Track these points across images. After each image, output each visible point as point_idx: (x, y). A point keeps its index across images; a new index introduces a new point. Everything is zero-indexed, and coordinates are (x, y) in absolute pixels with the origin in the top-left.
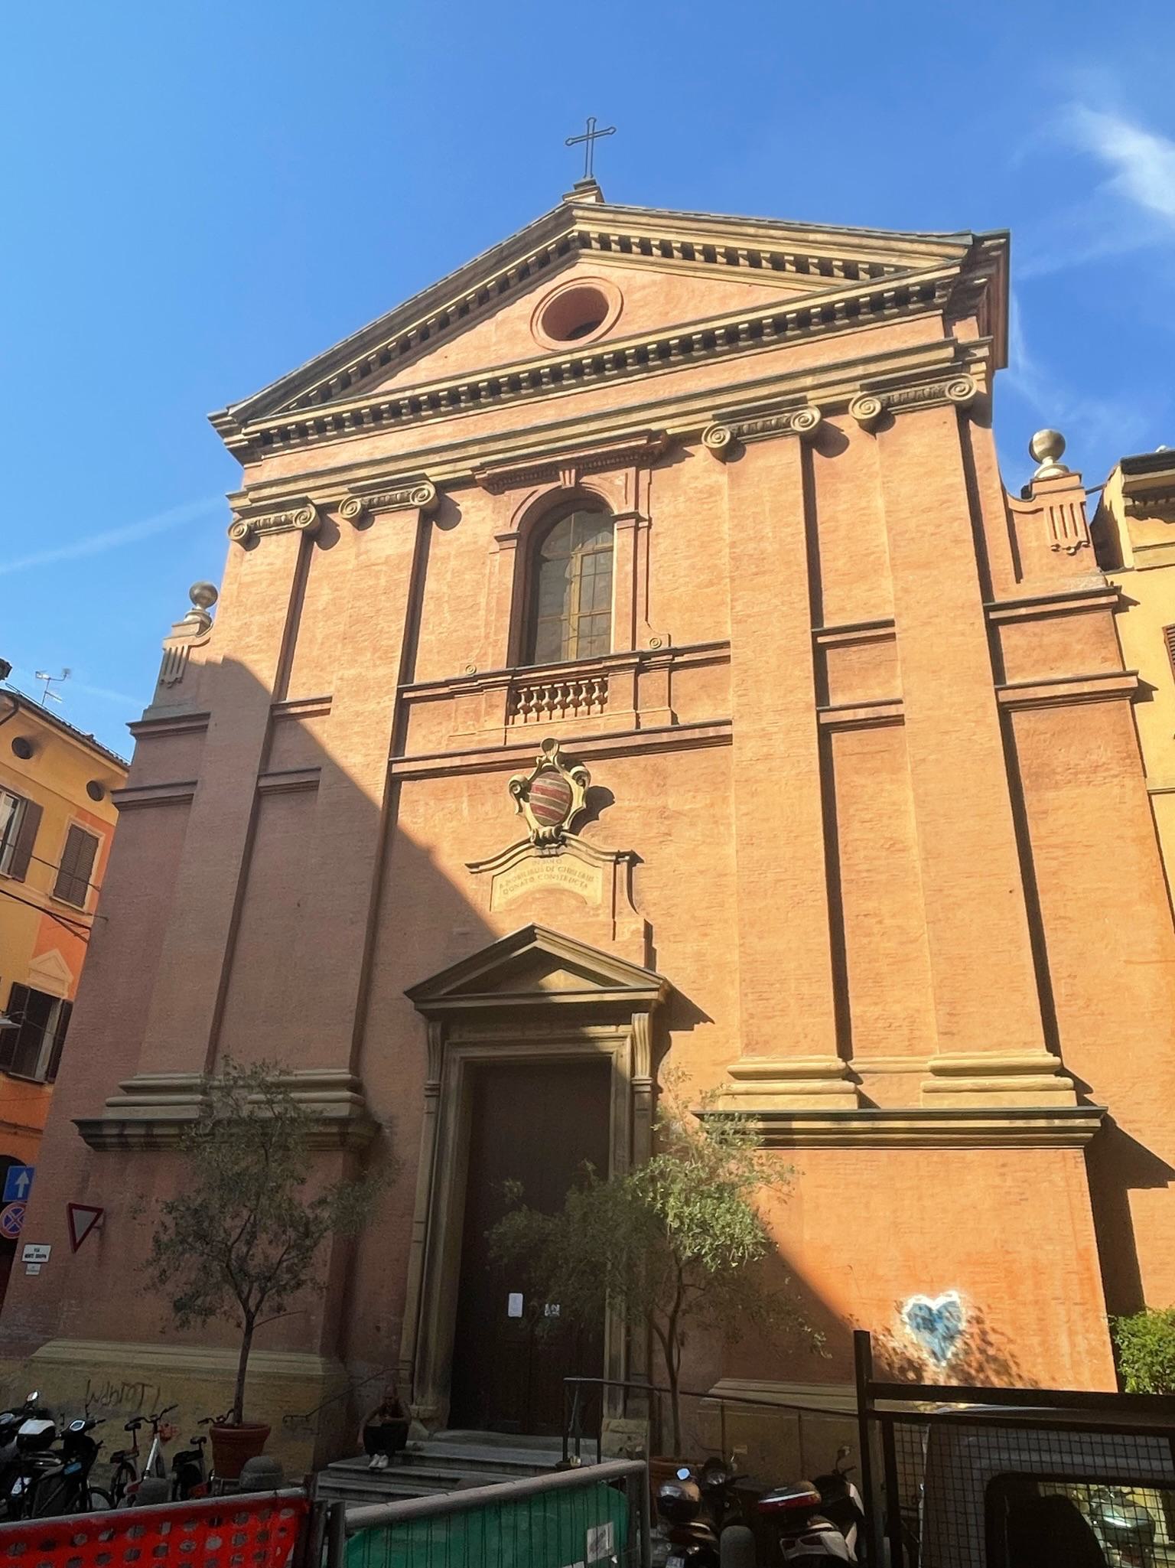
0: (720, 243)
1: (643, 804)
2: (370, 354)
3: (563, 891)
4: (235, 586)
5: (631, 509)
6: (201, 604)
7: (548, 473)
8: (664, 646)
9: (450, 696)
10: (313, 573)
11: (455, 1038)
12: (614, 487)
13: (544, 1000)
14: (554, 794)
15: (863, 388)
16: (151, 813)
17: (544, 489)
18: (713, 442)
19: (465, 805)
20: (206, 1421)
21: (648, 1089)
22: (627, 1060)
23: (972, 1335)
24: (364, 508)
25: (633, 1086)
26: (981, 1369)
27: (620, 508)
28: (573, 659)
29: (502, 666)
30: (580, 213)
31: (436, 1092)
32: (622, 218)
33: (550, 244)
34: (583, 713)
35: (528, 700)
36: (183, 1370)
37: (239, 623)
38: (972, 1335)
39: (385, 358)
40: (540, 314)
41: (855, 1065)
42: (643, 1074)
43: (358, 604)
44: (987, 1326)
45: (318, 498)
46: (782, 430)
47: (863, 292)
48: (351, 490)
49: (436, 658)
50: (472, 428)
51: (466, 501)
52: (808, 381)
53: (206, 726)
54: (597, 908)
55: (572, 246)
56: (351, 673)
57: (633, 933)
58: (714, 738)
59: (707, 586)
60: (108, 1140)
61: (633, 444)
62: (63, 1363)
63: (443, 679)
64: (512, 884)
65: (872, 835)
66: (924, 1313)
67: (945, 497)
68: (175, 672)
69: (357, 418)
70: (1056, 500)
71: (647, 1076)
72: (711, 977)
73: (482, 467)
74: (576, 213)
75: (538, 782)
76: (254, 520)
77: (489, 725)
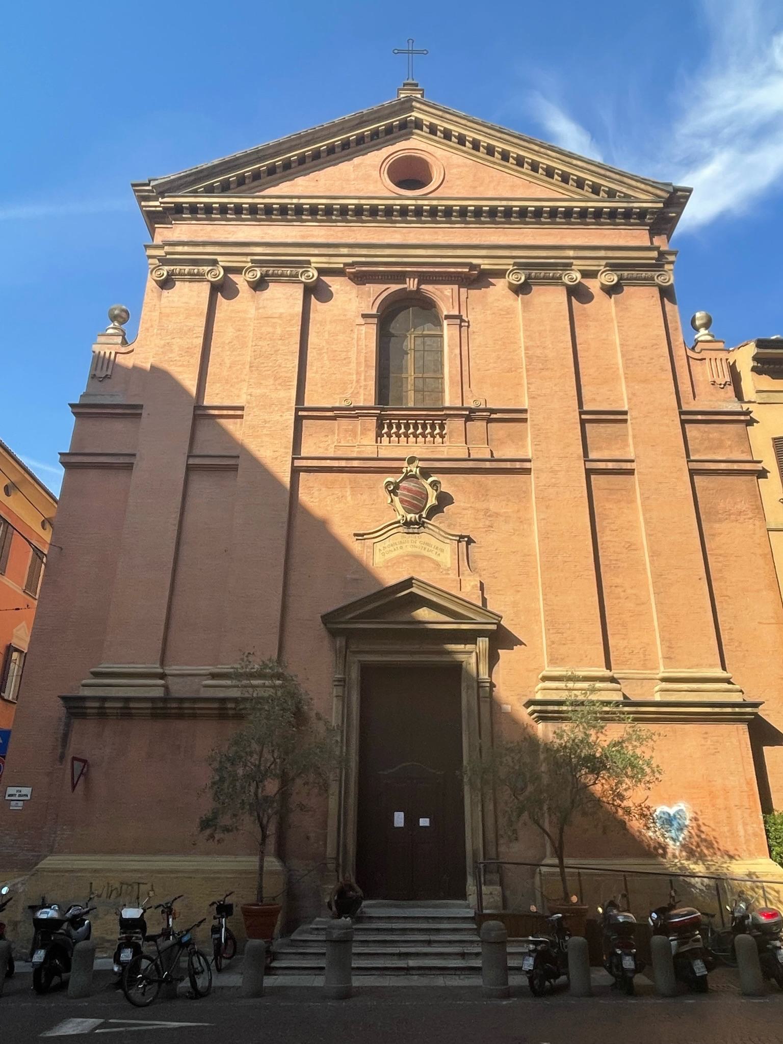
0: (514, 151)
1: (473, 505)
2: (263, 166)
3: (423, 557)
4: (157, 313)
5: (457, 313)
6: (119, 322)
7: (399, 277)
8: (483, 406)
10: (219, 315)
11: (353, 648)
12: (445, 297)
13: (421, 626)
14: (416, 493)
15: (606, 266)
16: (93, 474)
17: (394, 287)
18: (512, 279)
19: (348, 493)
20: (160, 906)
21: (488, 685)
22: (474, 666)
23: (692, 827)
24: (262, 276)
25: (478, 683)
26: (698, 846)
27: (448, 310)
28: (411, 405)
29: (371, 403)
30: (418, 105)
31: (342, 683)
32: (448, 116)
33: (395, 121)
34: (430, 442)
35: (398, 427)
36: (171, 872)
37: (162, 342)
38: (692, 827)
39: (272, 170)
40: (386, 167)
41: (615, 673)
42: (484, 675)
43: (260, 343)
44: (700, 822)
45: (223, 261)
46: (556, 281)
47: (607, 205)
48: (253, 261)
49: (320, 390)
50: (339, 235)
51: (335, 284)
52: (571, 253)
53: (141, 414)
54: (448, 570)
55: (409, 125)
56: (258, 391)
57: (474, 587)
58: (518, 469)
59: (508, 372)
60: (89, 711)
61: (459, 270)
62: (67, 871)
63: (329, 406)
64: (388, 549)
65: (617, 539)
66: (666, 816)
67: (654, 342)
68: (103, 370)
69: (253, 210)
70: (713, 354)
71: (487, 677)
72: (523, 618)
73: (353, 264)
74: (414, 104)
76: (172, 268)
77: (365, 442)
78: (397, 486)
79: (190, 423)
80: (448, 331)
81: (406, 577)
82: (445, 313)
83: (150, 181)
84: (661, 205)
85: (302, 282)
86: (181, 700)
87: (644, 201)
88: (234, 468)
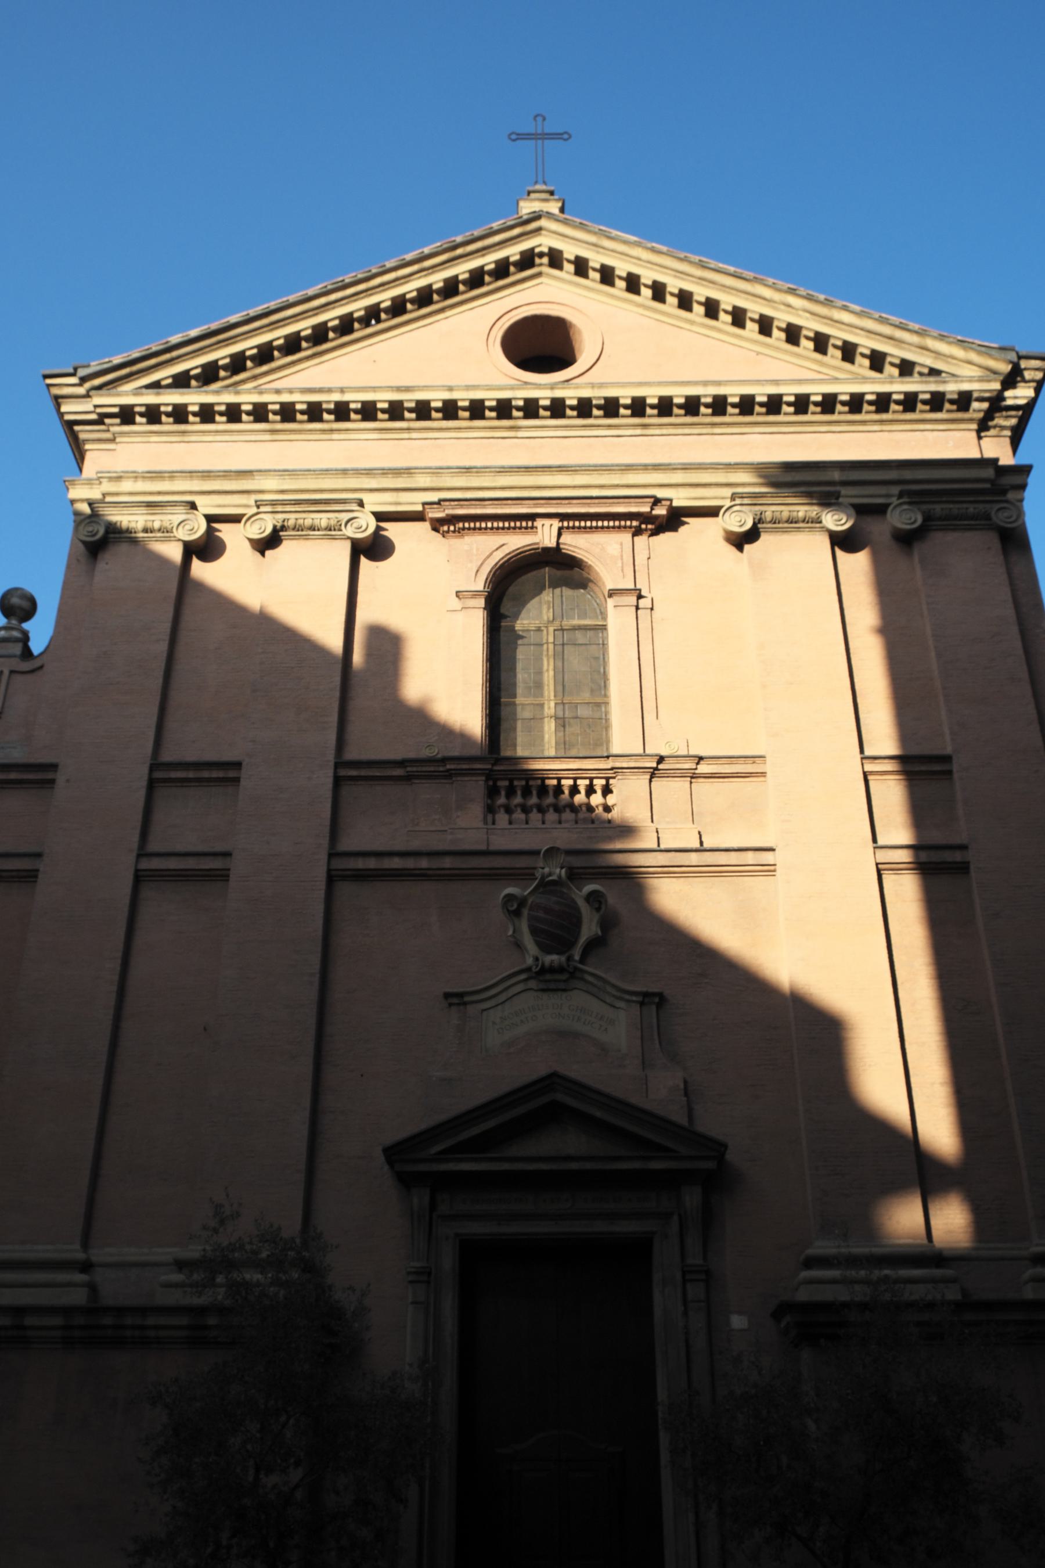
8: (683, 752)
9: (408, 778)
31: (424, 1276)
45: (208, 505)
53: (52, 782)
55: (537, 261)
78: (522, 902)
79: (142, 793)
80: (618, 619)
81: (543, 1071)
82: (610, 585)
83: (76, 369)
85: (349, 538)
86: (120, 1311)
88: (222, 876)
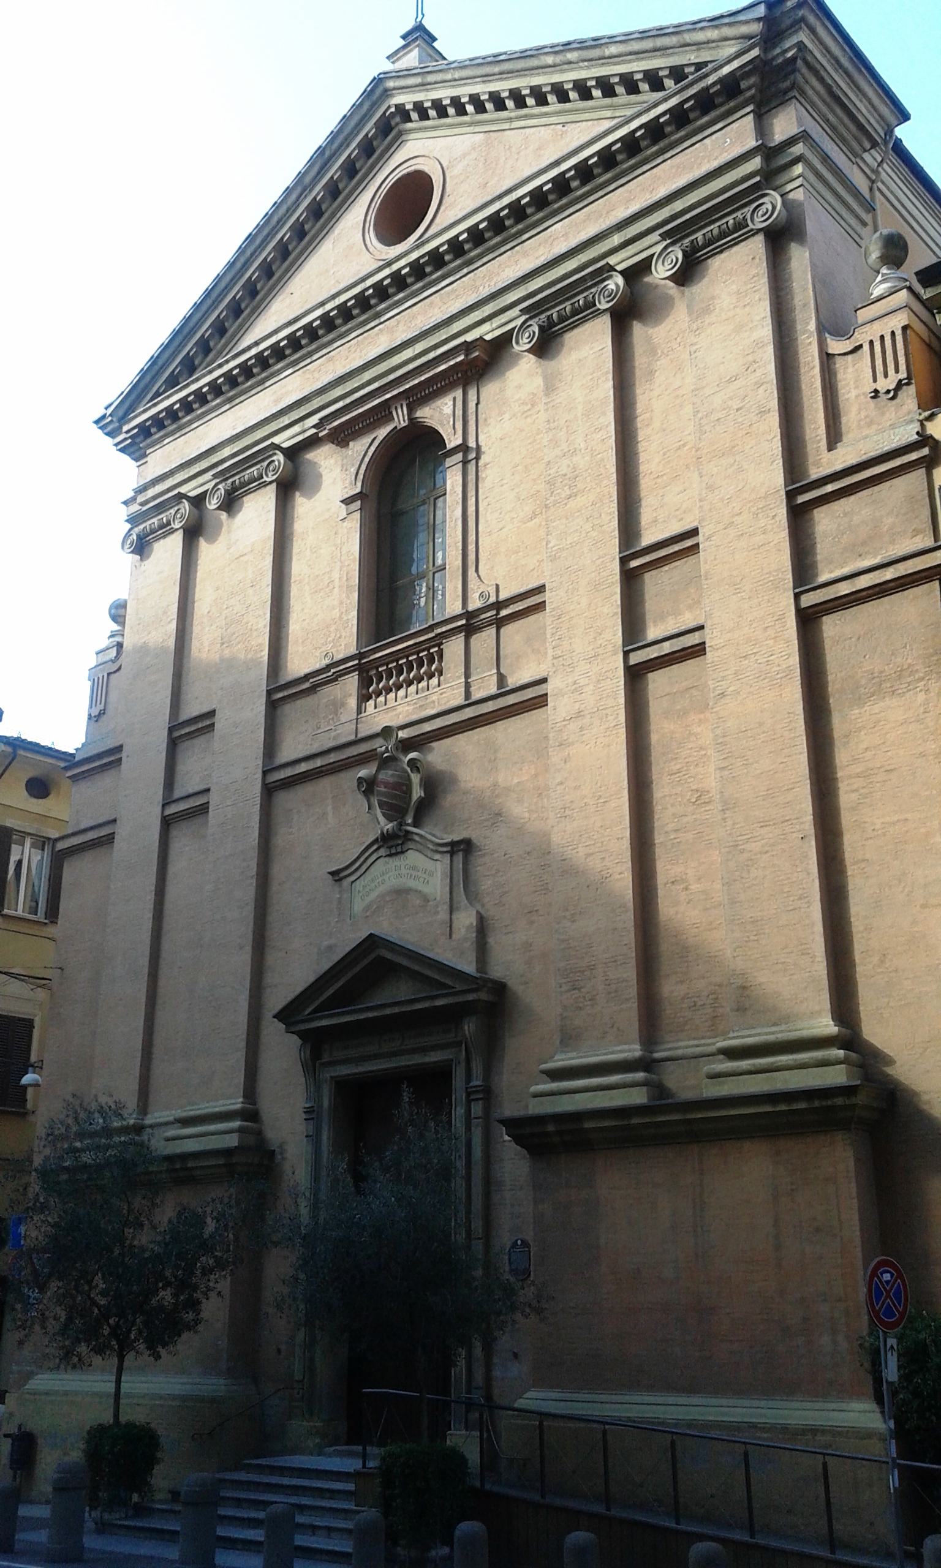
7: (382, 414)
15: (664, 236)
17: (383, 432)
19: (329, 809)
67: (750, 358)
75: (381, 776)
76: (141, 527)
84: (755, 52)
87: (728, 57)
